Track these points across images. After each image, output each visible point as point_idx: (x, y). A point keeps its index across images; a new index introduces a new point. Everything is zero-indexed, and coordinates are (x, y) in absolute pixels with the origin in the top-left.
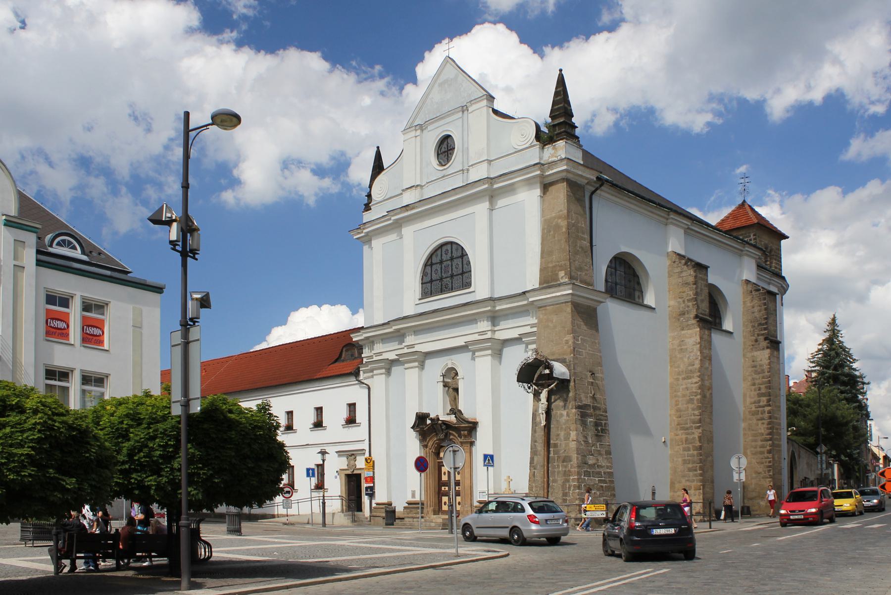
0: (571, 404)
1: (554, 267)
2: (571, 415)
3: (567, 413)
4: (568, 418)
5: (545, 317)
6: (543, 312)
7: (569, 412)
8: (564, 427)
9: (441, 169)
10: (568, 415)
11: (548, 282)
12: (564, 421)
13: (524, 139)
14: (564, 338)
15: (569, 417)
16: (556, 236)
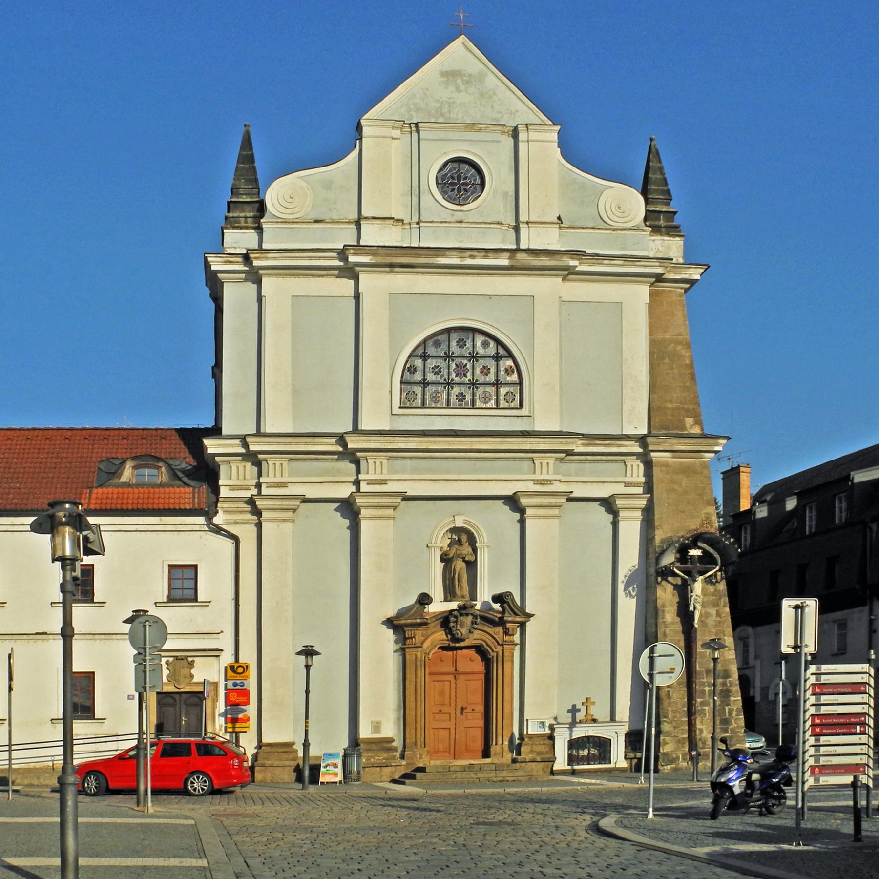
0: (722, 600)
1: (678, 408)
2: (723, 615)
3: (717, 611)
4: (718, 619)
5: (667, 476)
6: (664, 469)
7: (721, 611)
8: (714, 631)
9: (455, 209)
10: (718, 614)
11: (667, 428)
12: (713, 623)
13: (620, 215)
14: (702, 510)
15: (721, 618)
16: (675, 366)
